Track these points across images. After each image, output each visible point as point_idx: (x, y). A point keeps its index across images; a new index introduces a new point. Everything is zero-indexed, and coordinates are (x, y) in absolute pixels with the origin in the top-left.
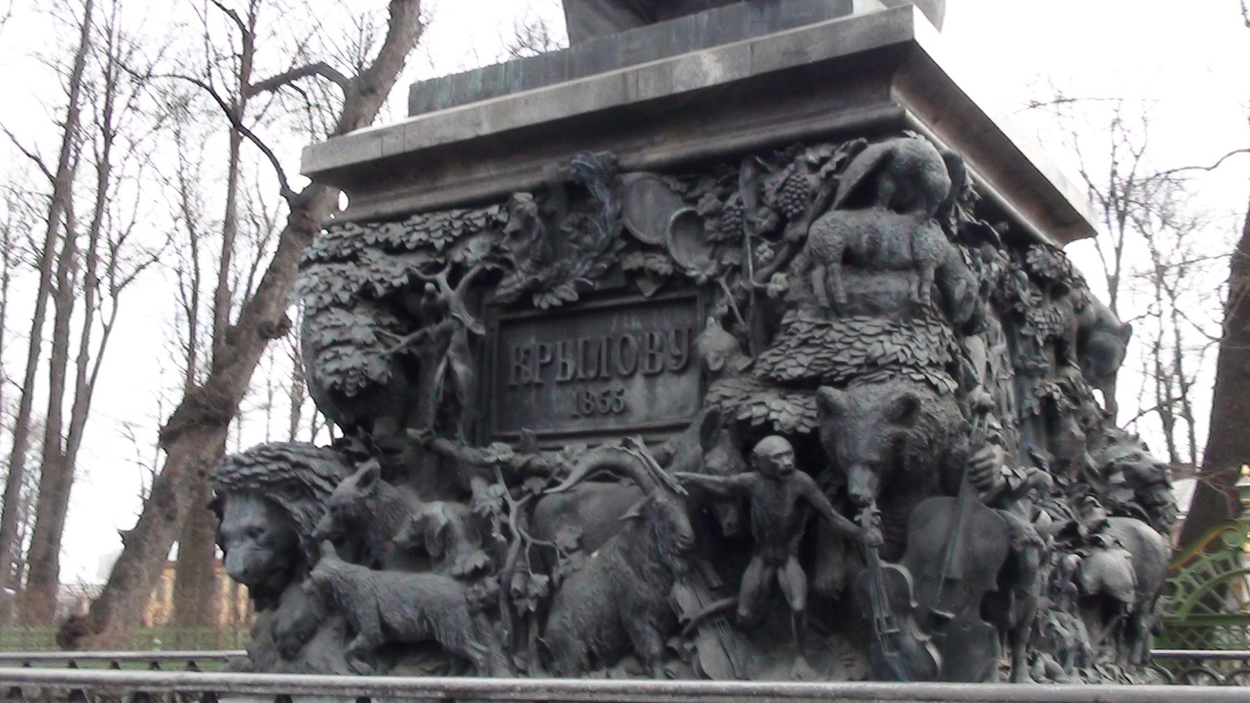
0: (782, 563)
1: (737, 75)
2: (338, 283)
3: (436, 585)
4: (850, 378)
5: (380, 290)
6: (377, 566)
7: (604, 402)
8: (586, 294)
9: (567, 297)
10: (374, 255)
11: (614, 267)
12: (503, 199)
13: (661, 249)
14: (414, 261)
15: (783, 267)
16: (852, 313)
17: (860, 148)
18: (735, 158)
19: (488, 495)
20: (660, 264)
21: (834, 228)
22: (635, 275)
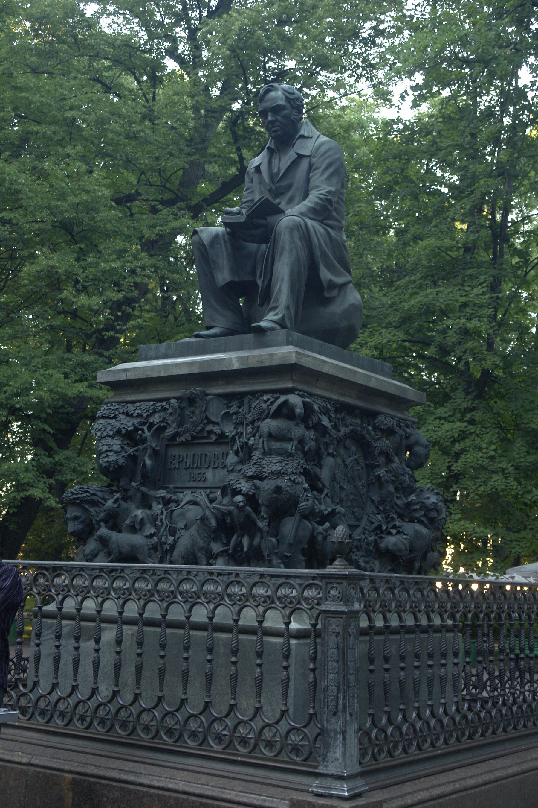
0: (243, 536)
1: (242, 367)
3: (138, 539)
4: (266, 477)
5: (124, 431)
6: (120, 532)
8: (194, 438)
10: (123, 417)
11: (203, 429)
12: (167, 400)
13: (217, 424)
14: (136, 421)
15: (254, 436)
16: (271, 454)
17: (279, 397)
19: (157, 508)
21: (269, 425)
22: (210, 432)
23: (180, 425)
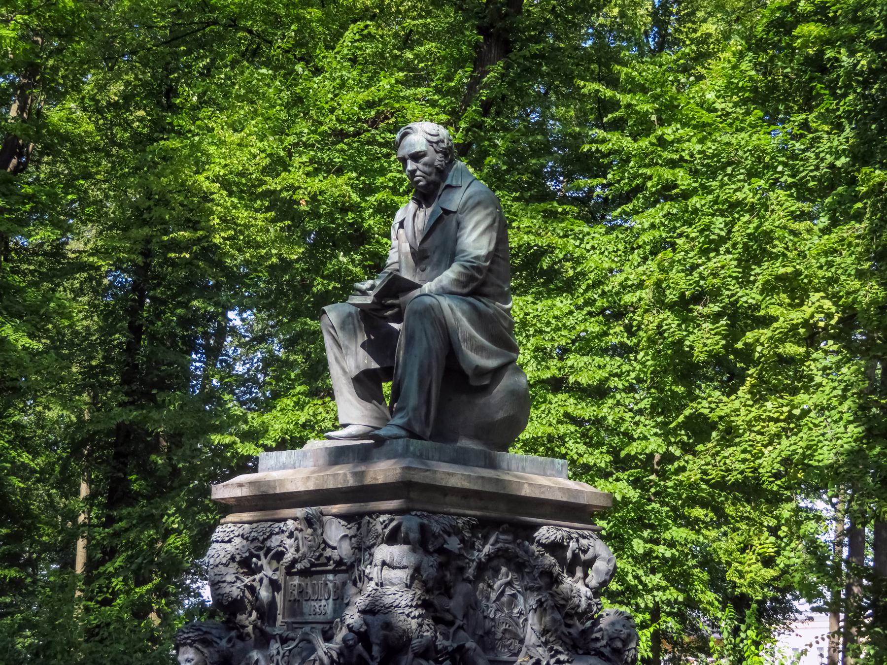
8: (313, 565)
11: (321, 555)
22: (329, 559)
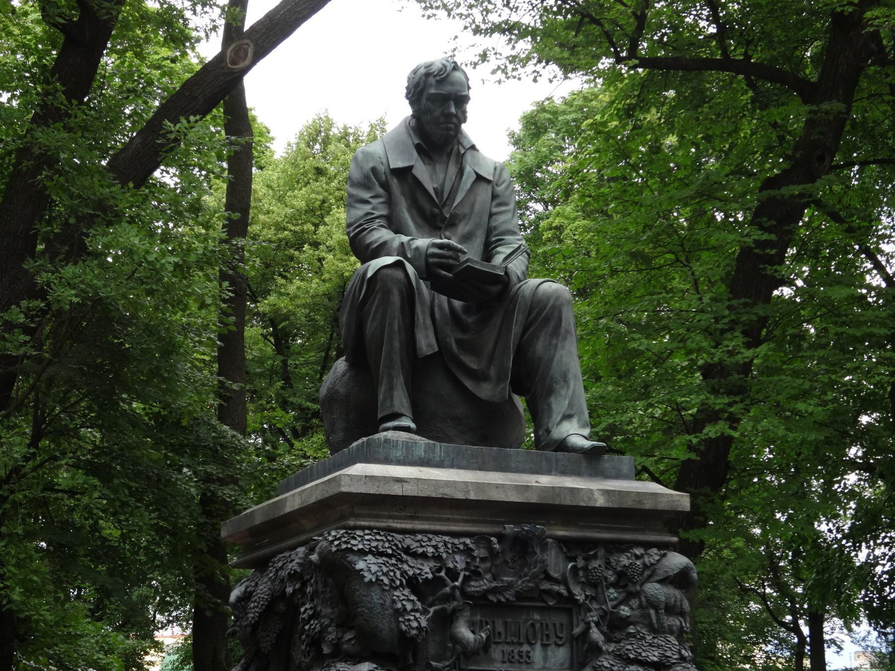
1: (611, 505)
2: (398, 573)
4: (674, 663)
7: (521, 657)
9: (511, 598)
18: (595, 543)
20: (562, 590)
23: (495, 578)
